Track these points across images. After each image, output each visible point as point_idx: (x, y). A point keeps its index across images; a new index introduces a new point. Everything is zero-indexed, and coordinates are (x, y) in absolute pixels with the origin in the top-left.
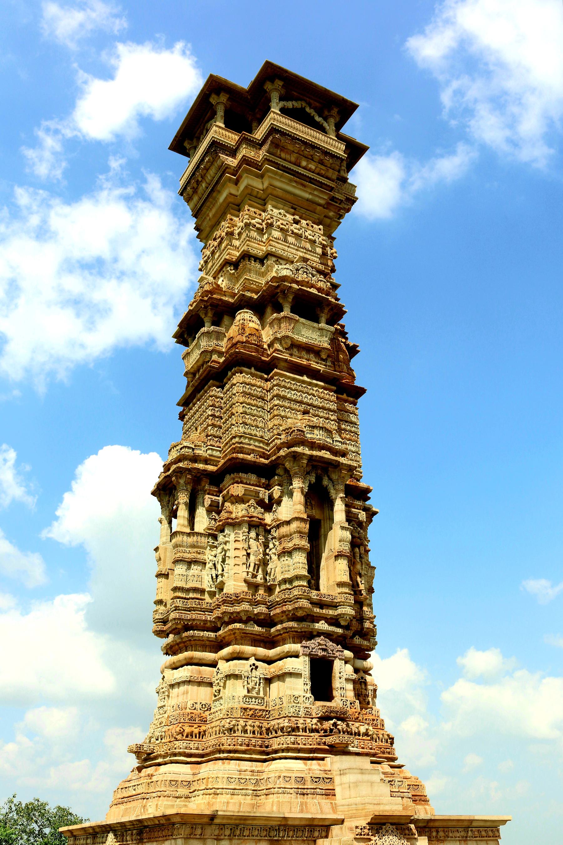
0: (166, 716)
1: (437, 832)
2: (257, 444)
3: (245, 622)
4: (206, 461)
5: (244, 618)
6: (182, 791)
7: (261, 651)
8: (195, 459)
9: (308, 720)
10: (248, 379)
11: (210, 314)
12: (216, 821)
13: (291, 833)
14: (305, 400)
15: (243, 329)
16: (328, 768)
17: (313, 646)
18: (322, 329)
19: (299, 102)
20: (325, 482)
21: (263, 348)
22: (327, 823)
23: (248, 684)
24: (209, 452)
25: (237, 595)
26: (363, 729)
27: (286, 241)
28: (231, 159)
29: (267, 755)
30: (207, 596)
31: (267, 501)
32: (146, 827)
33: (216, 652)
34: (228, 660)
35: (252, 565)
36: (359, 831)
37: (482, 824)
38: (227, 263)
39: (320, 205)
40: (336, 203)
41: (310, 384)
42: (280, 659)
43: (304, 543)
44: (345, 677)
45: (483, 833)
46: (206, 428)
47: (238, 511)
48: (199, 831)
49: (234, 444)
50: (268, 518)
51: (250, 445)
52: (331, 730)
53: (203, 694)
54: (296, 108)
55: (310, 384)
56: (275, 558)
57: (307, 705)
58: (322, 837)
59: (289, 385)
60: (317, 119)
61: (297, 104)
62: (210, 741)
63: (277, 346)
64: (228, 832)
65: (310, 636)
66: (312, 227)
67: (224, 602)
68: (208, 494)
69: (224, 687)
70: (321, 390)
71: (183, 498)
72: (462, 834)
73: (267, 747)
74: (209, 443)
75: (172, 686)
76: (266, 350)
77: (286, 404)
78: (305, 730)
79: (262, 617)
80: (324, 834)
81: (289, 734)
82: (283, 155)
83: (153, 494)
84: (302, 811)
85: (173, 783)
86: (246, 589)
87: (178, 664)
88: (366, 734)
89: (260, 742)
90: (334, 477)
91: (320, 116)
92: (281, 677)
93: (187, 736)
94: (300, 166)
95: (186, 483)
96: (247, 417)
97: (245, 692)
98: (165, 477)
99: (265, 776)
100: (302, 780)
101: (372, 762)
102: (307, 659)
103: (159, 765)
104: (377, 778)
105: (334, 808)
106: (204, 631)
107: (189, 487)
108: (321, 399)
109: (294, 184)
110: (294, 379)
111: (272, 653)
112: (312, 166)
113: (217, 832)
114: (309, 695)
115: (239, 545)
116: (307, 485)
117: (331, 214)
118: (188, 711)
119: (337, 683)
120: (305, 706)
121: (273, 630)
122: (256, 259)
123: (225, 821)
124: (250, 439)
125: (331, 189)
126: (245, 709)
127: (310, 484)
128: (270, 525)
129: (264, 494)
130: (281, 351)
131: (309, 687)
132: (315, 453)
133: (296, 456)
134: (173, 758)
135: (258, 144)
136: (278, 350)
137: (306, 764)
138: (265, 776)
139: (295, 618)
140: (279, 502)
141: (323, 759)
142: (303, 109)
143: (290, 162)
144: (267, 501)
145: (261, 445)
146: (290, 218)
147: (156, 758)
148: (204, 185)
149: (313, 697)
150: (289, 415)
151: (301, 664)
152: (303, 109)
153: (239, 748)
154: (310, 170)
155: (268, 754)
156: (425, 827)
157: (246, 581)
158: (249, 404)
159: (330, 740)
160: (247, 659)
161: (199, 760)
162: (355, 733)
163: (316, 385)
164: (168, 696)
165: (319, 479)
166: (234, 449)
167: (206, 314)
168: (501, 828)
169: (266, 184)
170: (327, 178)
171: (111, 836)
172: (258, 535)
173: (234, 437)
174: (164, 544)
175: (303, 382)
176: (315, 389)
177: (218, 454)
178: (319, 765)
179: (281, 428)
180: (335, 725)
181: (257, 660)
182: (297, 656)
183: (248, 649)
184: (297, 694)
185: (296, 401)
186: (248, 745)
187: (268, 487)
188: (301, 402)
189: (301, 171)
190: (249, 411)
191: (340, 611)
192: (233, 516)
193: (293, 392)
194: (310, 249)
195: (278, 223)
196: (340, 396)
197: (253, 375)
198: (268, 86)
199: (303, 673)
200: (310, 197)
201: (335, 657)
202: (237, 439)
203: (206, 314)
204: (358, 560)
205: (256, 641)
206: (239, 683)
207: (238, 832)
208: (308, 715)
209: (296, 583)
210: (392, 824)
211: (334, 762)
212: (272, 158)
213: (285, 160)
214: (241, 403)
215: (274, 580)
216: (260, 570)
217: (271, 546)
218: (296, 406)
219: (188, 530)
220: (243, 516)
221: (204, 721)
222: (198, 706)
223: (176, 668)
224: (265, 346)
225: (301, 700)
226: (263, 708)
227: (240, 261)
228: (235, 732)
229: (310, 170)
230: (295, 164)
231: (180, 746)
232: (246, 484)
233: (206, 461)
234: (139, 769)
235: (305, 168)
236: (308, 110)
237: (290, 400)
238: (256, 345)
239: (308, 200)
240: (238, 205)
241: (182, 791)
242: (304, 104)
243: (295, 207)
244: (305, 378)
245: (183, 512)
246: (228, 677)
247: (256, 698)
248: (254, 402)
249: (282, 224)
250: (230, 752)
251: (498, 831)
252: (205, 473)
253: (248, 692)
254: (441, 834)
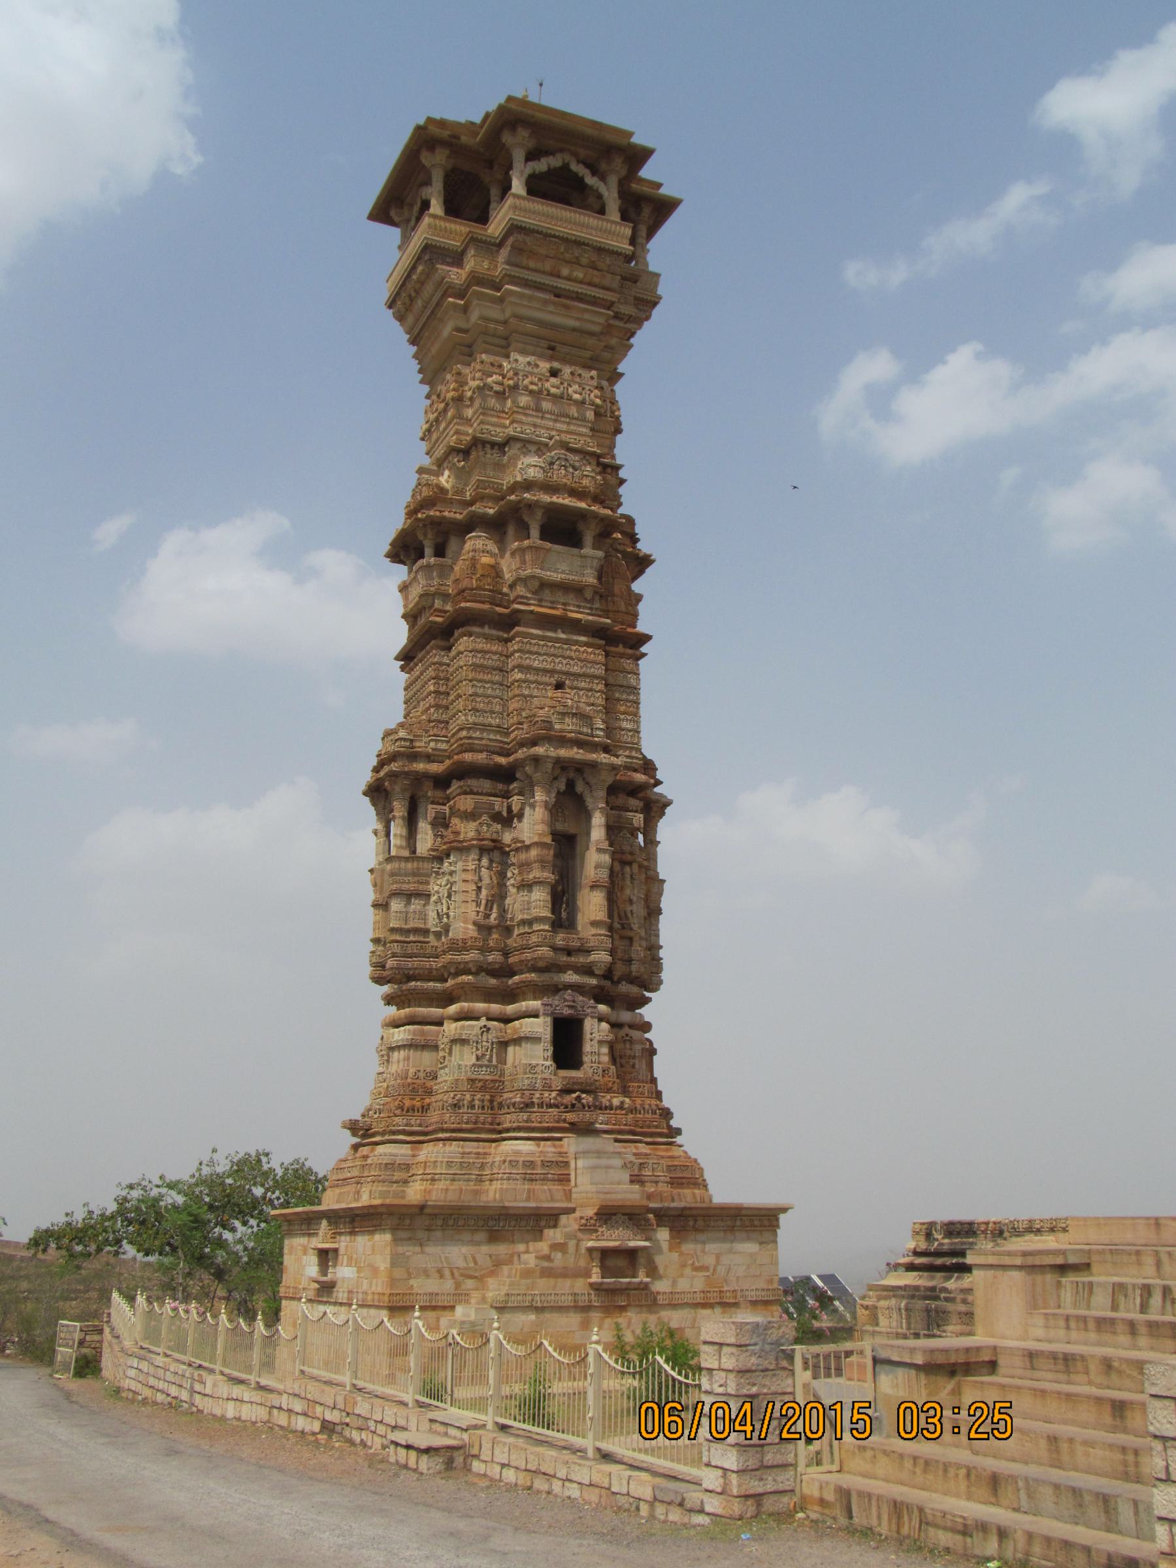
0: (385, 1085)
1: (696, 1221)
2: (492, 737)
3: (476, 974)
4: (429, 758)
5: (473, 970)
6: (398, 1175)
7: (495, 1008)
8: (414, 757)
9: (546, 1094)
10: (482, 644)
11: (430, 536)
12: (427, 1211)
13: (513, 1223)
14: (559, 667)
15: (474, 566)
16: (565, 1150)
17: (556, 1002)
18: (585, 557)
19: (559, 156)
20: (580, 787)
21: (501, 593)
22: (555, 1212)
23: (477, 1049)
24: (432, 744)
25: (464, 941)
26: (616, 1102)
27: (538, 409)
28: (455, 270)
29: (498, 1134)
30: (431, 938)
31: (505, 814)
32: (357, 1215)
33: (444, 1007)
34: (457, 1019)
35: (483, 902)
36: (583, 1221)
37: (755, 1212)
38: (452, 450)
39: (592, 334)
40: (621, 319)
42: (518, 1019)
43: (549, 876)
44: (598, 1038)
45: (756, 1223)
46: (428, 709)
47: (468, 830)
48: (407, 1222)
49: (461, 739)
50: (507, 838)
51: (482, 739)
52: (573, 1106)
53: (426, 1059)
54: (555, 169)
55: (566, 642)
56: (513, 890)
57: (546, 1075)
58: (550, 1227)
59: (535, 649)
60: (590, 180)
61: (555, 162)
62: (433, 1117)
63: (520, 590)
64: (440, 1222)
65: (556, 989)
66: (580, 375)
67: (450, 949)
68: (433, 803)
69: (450, 1053)
70: (582, 649)
71: (399, 809)
72: (729, 1223)
73: (499, 1124)
74: (431, 733)
75: (391, 1049)
76: (506, 595)
77: (531, 677)
78: (541, 1105)
79: (497, 966)
80: (552, 1223)
81: (521, 1110)
82: (532, 264)
83: (365, 794)
84: (528, 1199)
85: (390, 1166)
86: (475, 934)
87: (399, 1023)
88: (621, 1107)
89: (489, 1120)
90: (592, 781)
91: (594, 173)
92: (518, 1041)
93: (408, 1111)
94: (559, 277)
95: (403, 790)
96: (478, 699)
97: (473, 1060)
98: (378, 779)
99: (490, 1160)
100: (531, 1164)
101: (617, 1141)
102: (549, 1020)
103: (377, 1144)
104: (618, 1162)
105: (568, 1195)
106: (430, 980)
107: (407, 795)
108: (582, 661)
109: (551, 308)
110: (543, 638)
111: (510, 1009)
112: (579, 274)
113: (427, 1223)
114: (549, 1063)
115: (469, 877)
116: (553, 795)
117: (614, 341)
118: (409, 1080)
119: (588, 1047)
120: (544, 1076)
121: (510, 982)
122: (493, 445)
123: (436, 1211)
124: (482, 731)
125: (609, 306)
126: (473, 1081)
127: (558, 792)
128: (509, 846)
129: (499, 804)
130: (526, 598)
131: (550, 1053)
132: (563, 753)
133: (536, 760)
134: (392, 1136)
135: (494, 245)
136: (522, 597)
137: (539, 1146)
138: (490, 1160)
139: (534, 969)
140: (520, 816)
141: (560, 1139)
142: (565, 167)
143: (544, 272)
144: (505, 814)
145: (498, 737)
146: (544, 366)
147: (373, 1135)
148: (420, 302)
149: (554, 1065)
150: (535, 692)
151: (541, 1027)
152: (565, 167)
153: (464, 1126)
154: (575, 280)
155: (500, 1132)
156: (680, 1216)
157: (475, 923)
158: (480, 681)
159: (571, 1117)
160: (477, 1019)
161: (422, 1138)
162: (606, 1108)
164: (388, 1061)
165: (571, 785)
166: (462, 745)
167: (425, 535)
168: (782, 1217)
169: (508, 313)
170: (604, 288)
171: (324, 1223)
172: (491, 861)
173: (461, 729)
174: (380, 863)
175: (557, 640)
176: (574, 648)
177: (444, 746)
178: (555, 1146)
179: (524, 714)
180: (578, 1098)
181: (489, 1019)
182: (536, 1016)
183: (480, 1006)
184: (534, 1062)
185: (545, 671)
186: (475, 1123)
187: (506, 795)
188: (552, 672)
190: (480, 691)
191: (593, 957)
192: (461, 837)
193: (541, 658)
194: (576, 415)
195: (526, 382)
196: (613, 649)
197: (488, 638)
198: (507, 138)
199: (543, 1037)
200: (576, 324)
201: (586, 1015)
202: (464, 733)
203: (425, 535)
204: (628, 883)
205: (489, 996)
206: (466, 1048)
207: (451, 1222)
208: (548, 1087)
209: (536, 927)
210: (624, 1214)
211: (571, 1144)
212: (516, 271)
213: (536, 271)
214: (470, 681)
215: (512, 919)
216: (495, 906)
217: (509, 874)
218: (546, 679)
219: (406, 853)
220: (473, 839)
221: (429, 1092)
222: (421, 1075)
223: (397, 1027)
224: (505, 590)
225: (539, 1069)
226: (497, 1078)
227: (470, 448)
228: (459, 1108)
229: (575, 280)
230: (551, 274)
231: (399, 1122)
232: (477, 794)
233: (429, 758)
234: (356, 1147)
235: (568, 279)
236: (576, 168)
237: (537, 670)
238: (490, 591)
239: (574, 330)
240: (470, 346)
241: (398, 1175)
242: (567, 157)
243: (554, 346)
245: (397, 829)
246: (454, 1041)
247: (487, 1066)
248: (487, 677)
249: (532, 383)
250: (453, 1131)
251: (777, 1220)
252: (426, 776)
253: (478, 1059)
254: (700, 1223)
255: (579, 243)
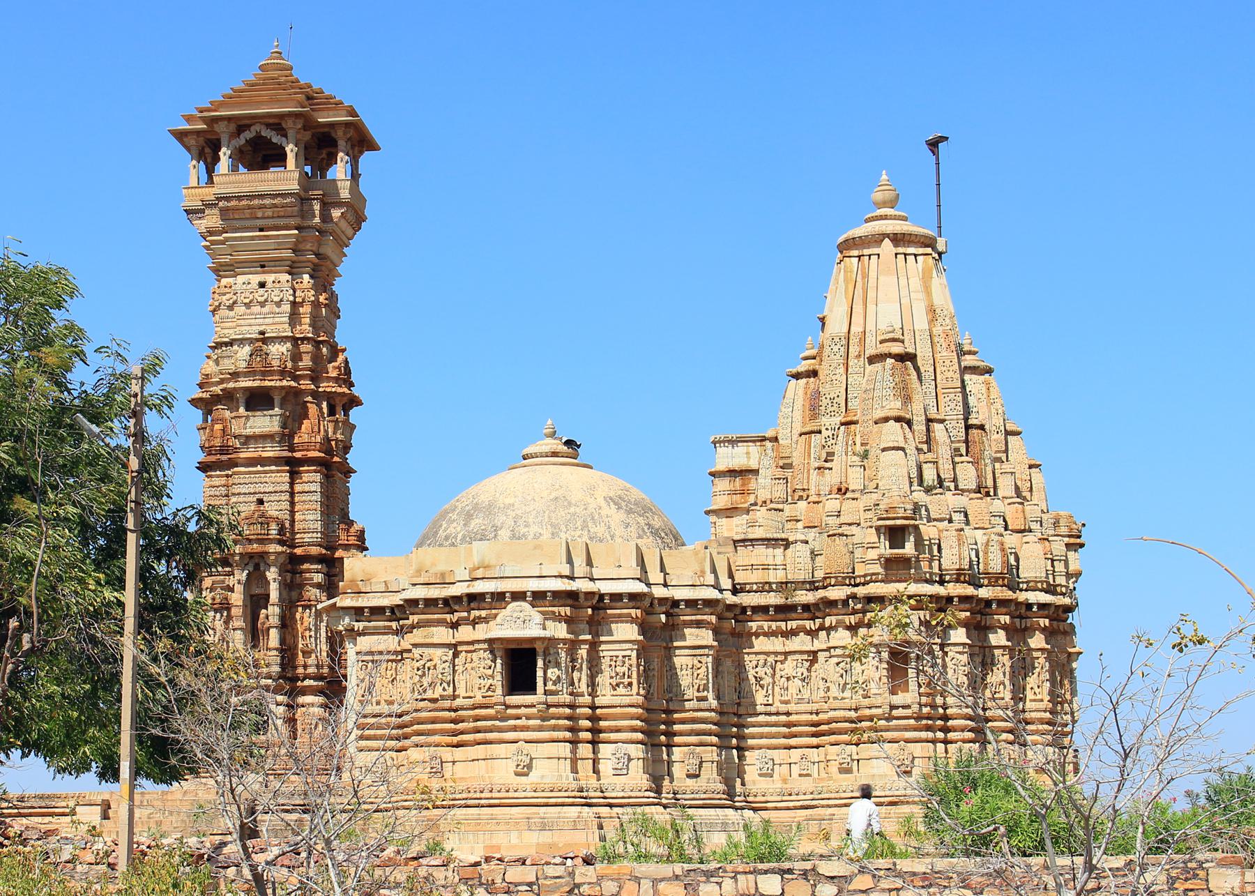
41: (265, 472)
55: (265, 472)
61: (248, 135)
77: (241, 499)
110: (250, 473)
146: (256, 279)
163: (272, 472)
165: (257, 567)
189: (259, 223)
236: (266, 133)
244: (259, 468)
255: (261, 196)
